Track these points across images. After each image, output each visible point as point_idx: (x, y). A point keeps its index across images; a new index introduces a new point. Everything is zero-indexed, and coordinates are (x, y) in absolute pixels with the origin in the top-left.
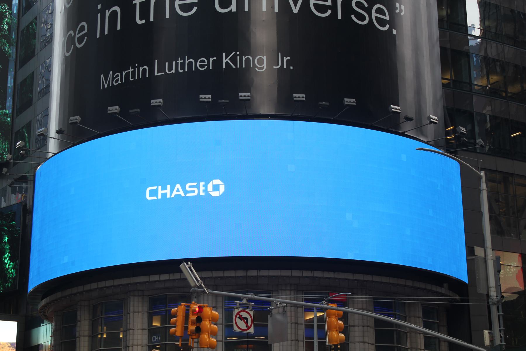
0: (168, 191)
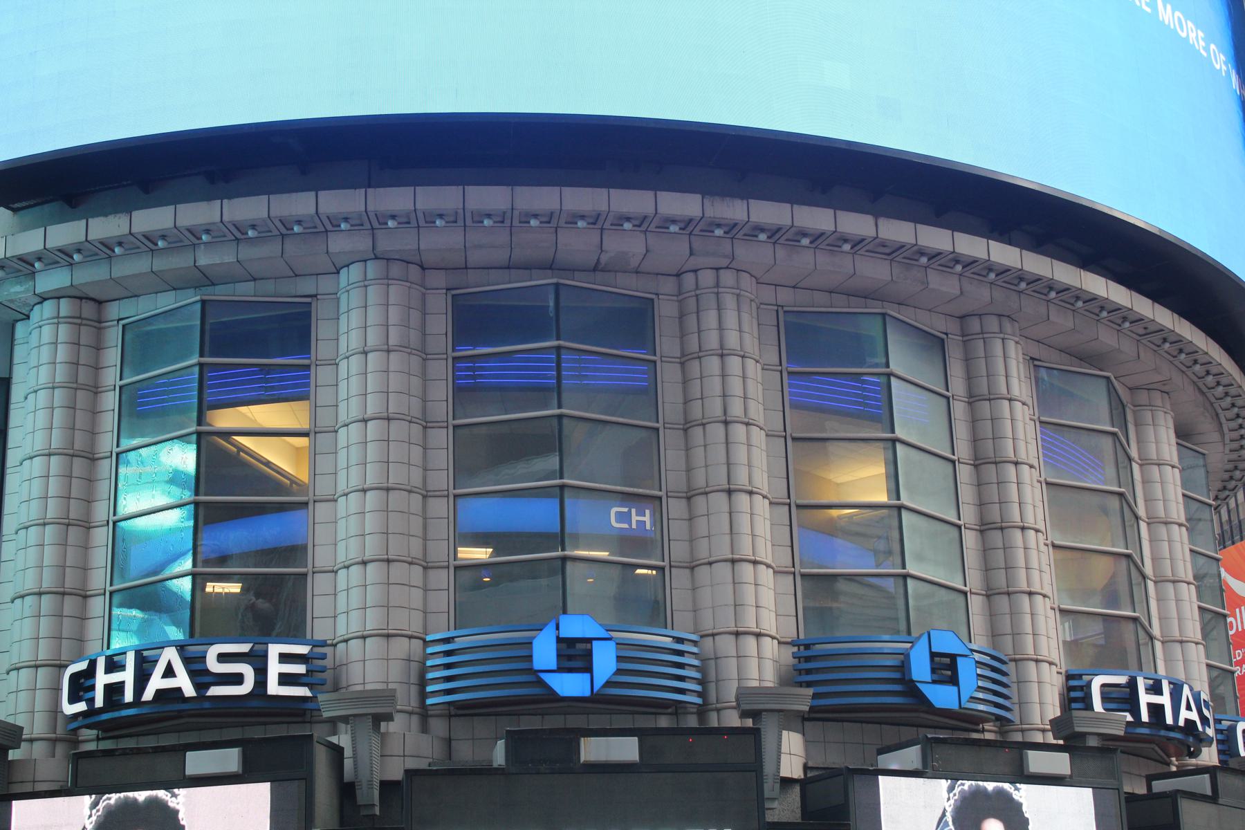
0: (127, 677)
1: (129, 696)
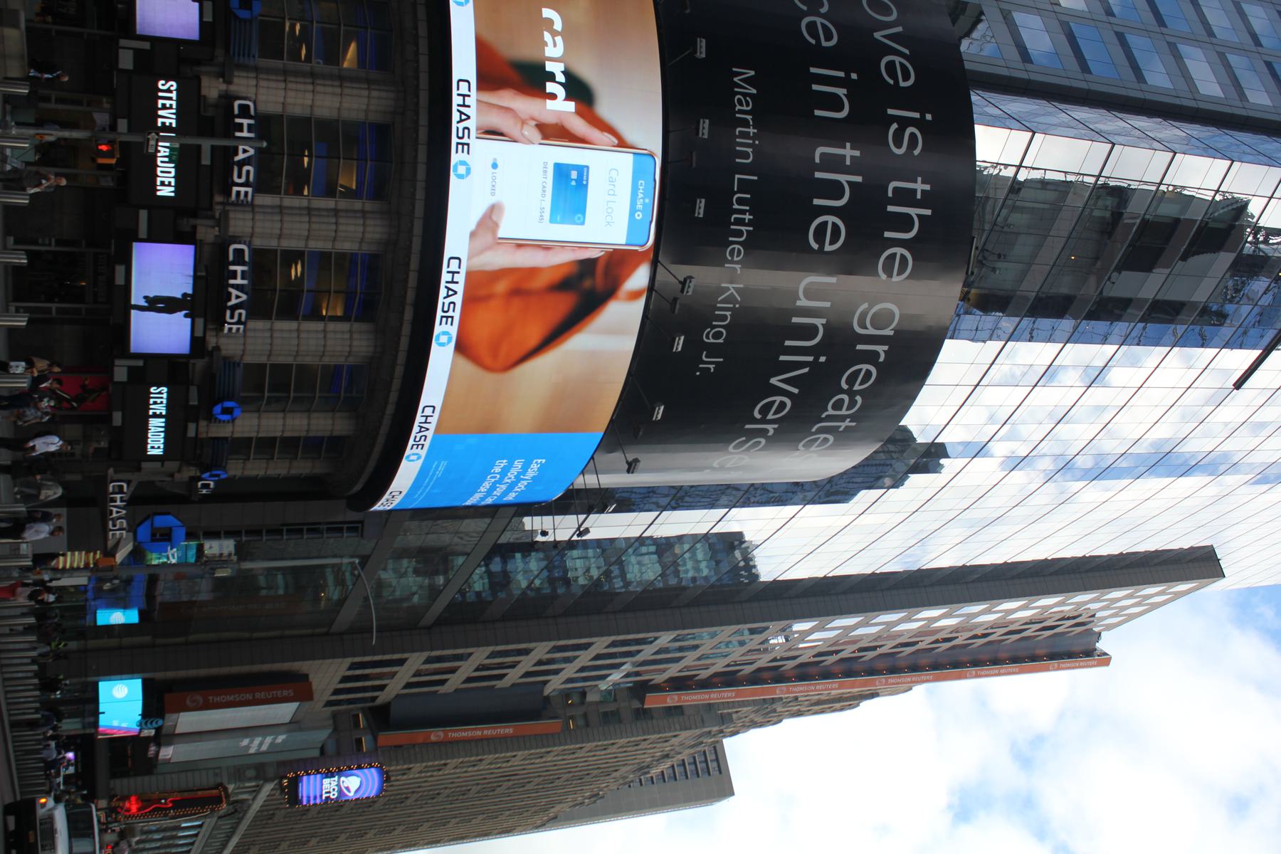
0: (239, 281)
1: (232, 282)
